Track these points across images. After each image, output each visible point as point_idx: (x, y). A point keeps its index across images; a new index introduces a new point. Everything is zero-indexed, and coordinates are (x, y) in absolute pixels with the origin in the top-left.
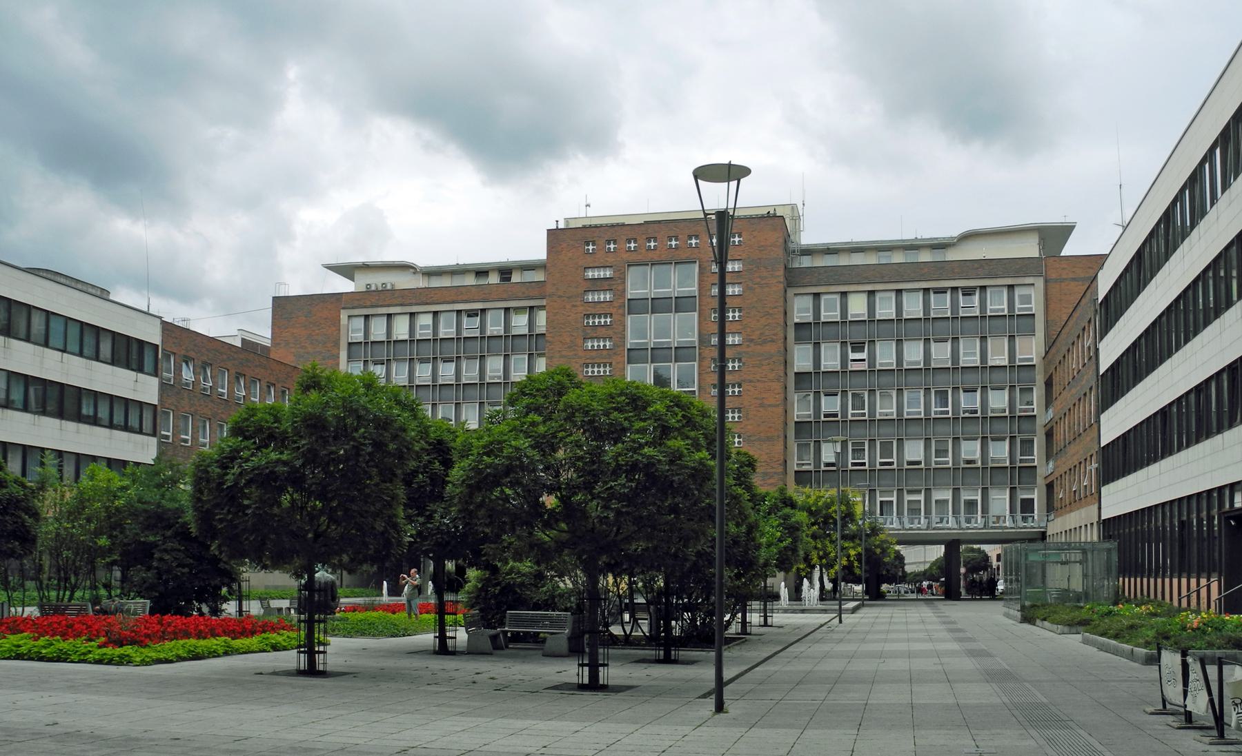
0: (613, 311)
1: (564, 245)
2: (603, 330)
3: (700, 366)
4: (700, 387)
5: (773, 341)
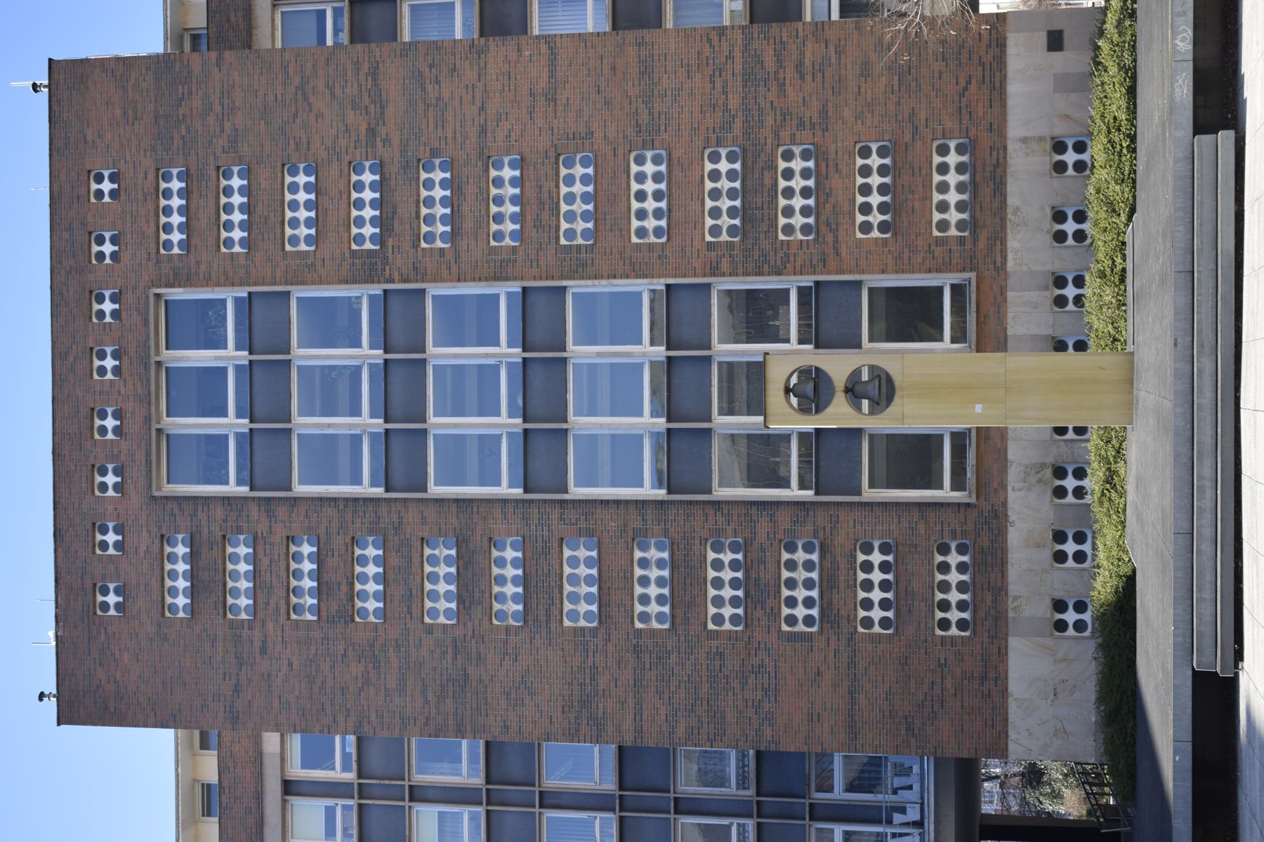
0: (280, 532)
2: (331, 562)
3: (437, 279)
4: (498, 276)
5: (374, 73)
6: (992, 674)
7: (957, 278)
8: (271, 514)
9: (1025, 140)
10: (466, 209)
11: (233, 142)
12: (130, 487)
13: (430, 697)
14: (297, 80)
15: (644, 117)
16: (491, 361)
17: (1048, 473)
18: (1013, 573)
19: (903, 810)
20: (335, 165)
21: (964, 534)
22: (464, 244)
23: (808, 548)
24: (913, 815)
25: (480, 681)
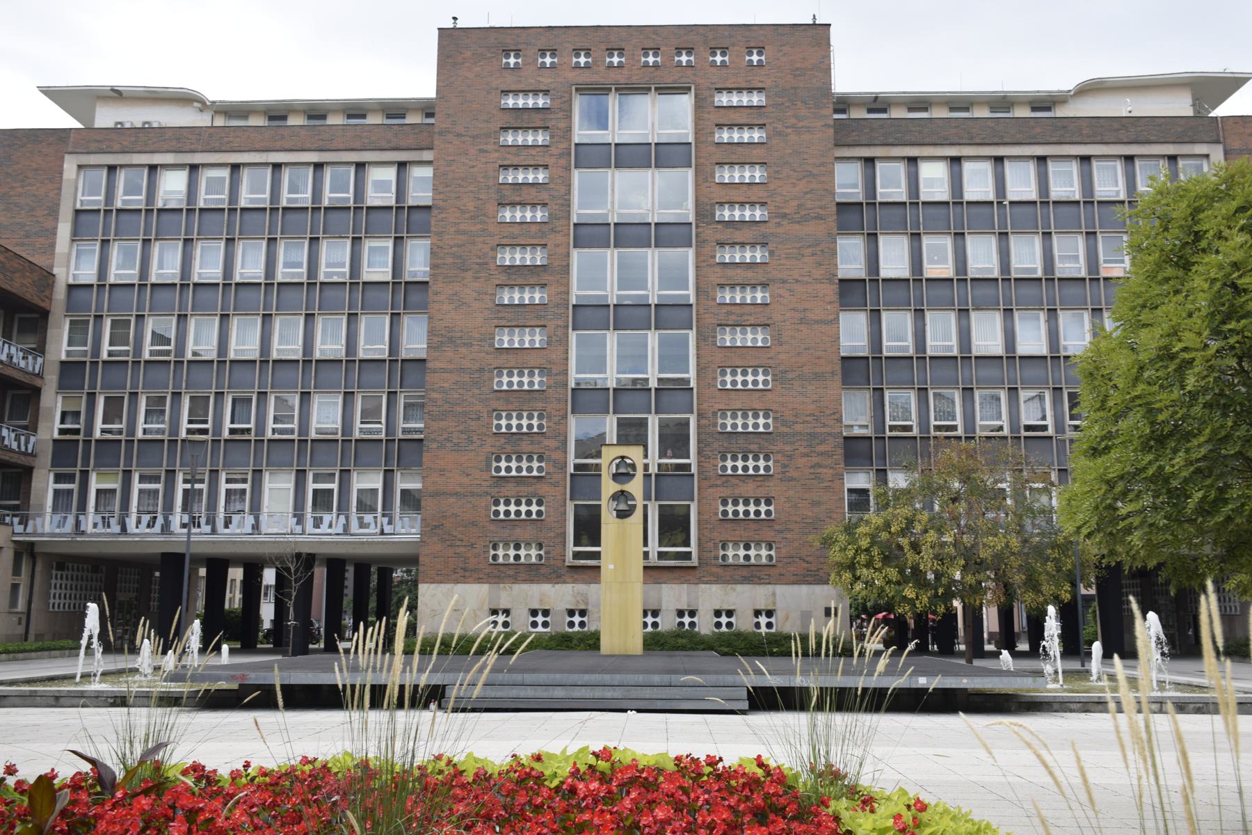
0: (550, 161)
1: (468, 54)
2: (533, 191)
3: (698, 254)
4: (698, 290)
5: (819, 217)
6: (467, 574)
7: (695, 556)
8: (561, 155)
9: (774, 594)
10: (739, 271)
11: (780, 134)
12: (578, 71)
13: (455, 249)
14: (815, 171)
15: (790, 376)
16: (650, 285)
17: (582, 607)
18: (525, 586)
19: (390, 523)
20: (765, 194)
21: (548, 559)
22: (718, 269)
23: (540, 469)
24: (387, 529)
25: (463, 278)
